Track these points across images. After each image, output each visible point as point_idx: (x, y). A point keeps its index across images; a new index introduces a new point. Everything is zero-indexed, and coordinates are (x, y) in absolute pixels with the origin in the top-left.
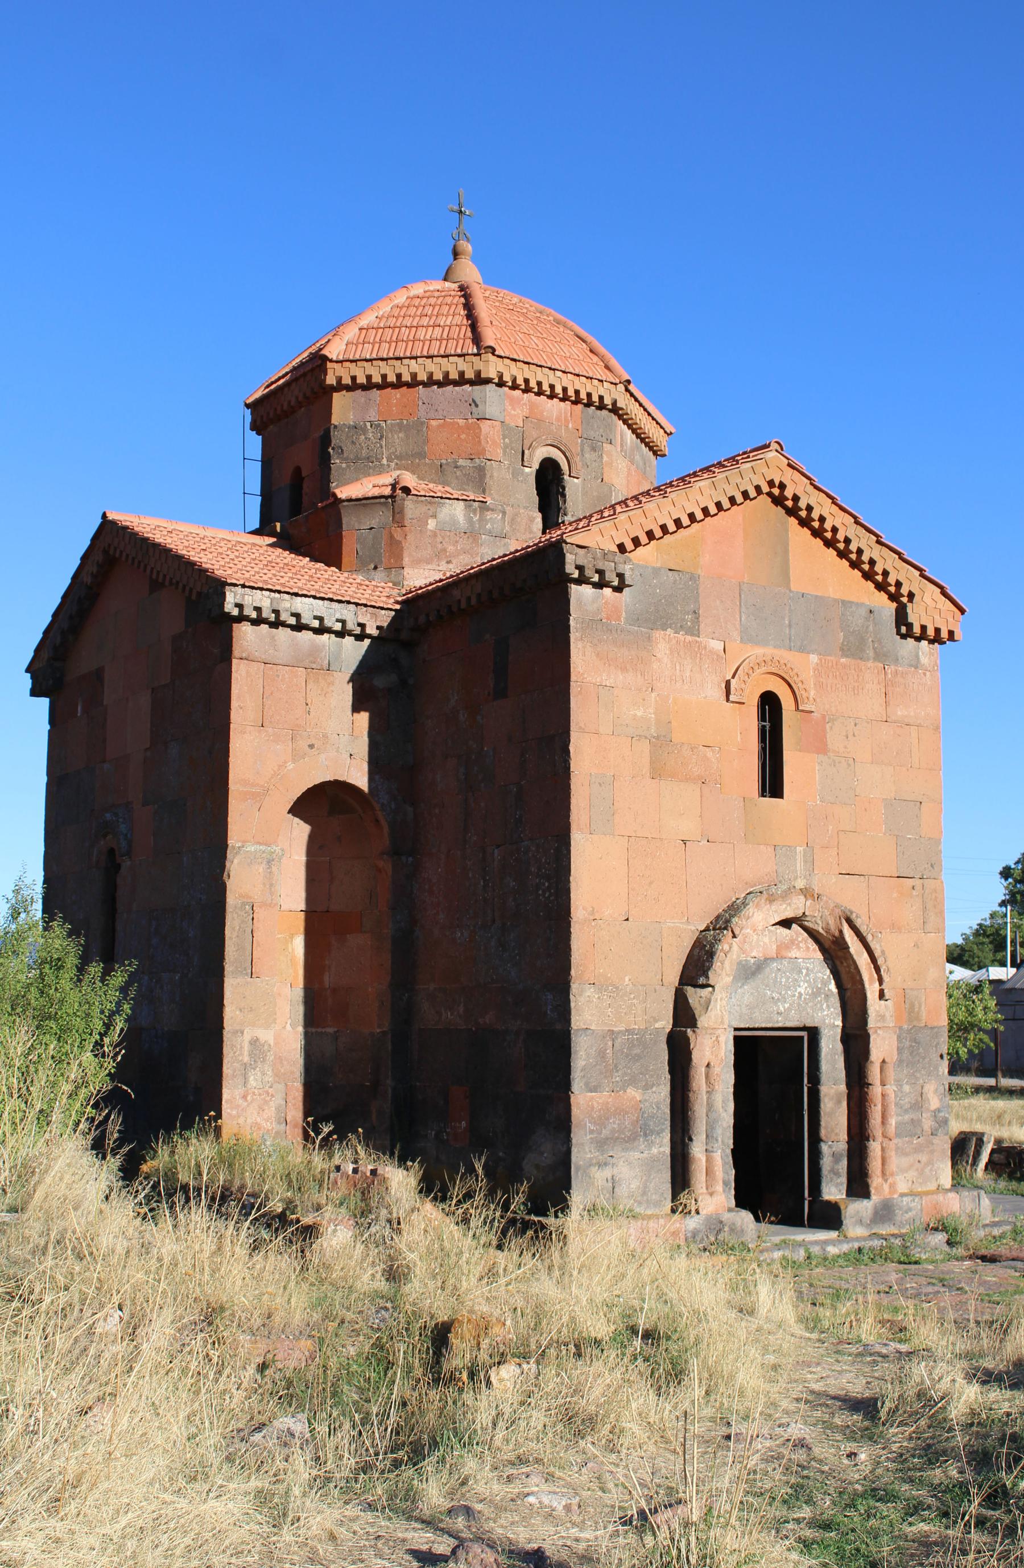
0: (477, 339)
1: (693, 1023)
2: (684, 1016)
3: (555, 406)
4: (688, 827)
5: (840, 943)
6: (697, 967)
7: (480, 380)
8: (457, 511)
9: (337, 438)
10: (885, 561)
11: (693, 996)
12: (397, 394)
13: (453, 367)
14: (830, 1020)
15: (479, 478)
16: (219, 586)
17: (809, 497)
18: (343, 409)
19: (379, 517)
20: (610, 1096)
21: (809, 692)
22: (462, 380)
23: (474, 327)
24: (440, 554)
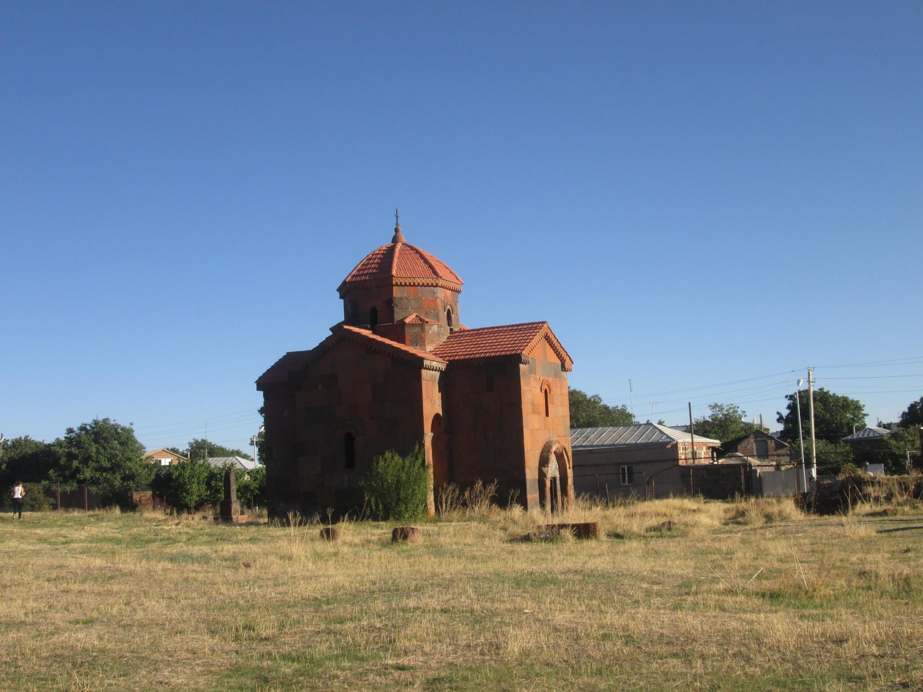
0: (435, 272)
1: (545, 476)
2: (542, 475)
3: (449, 292)
4: (537, 426)
5: (562, 455)
6: (544, 461)
7: (437, 286)
8: (435, 328)
9: (396, 302)
10: (562, 352)
11: (544, 469)
12: (412, 289)
13: (430, 281)
14: (557, 475)
15: (437, 317)
16: (421, 359)
17: (551, 336)
18: (397, 292)
19: (417, 330)
20: (532, 495)
21: (552, 388)
22: (432, 285)
23: (431, 267)
24: (433, 341)
